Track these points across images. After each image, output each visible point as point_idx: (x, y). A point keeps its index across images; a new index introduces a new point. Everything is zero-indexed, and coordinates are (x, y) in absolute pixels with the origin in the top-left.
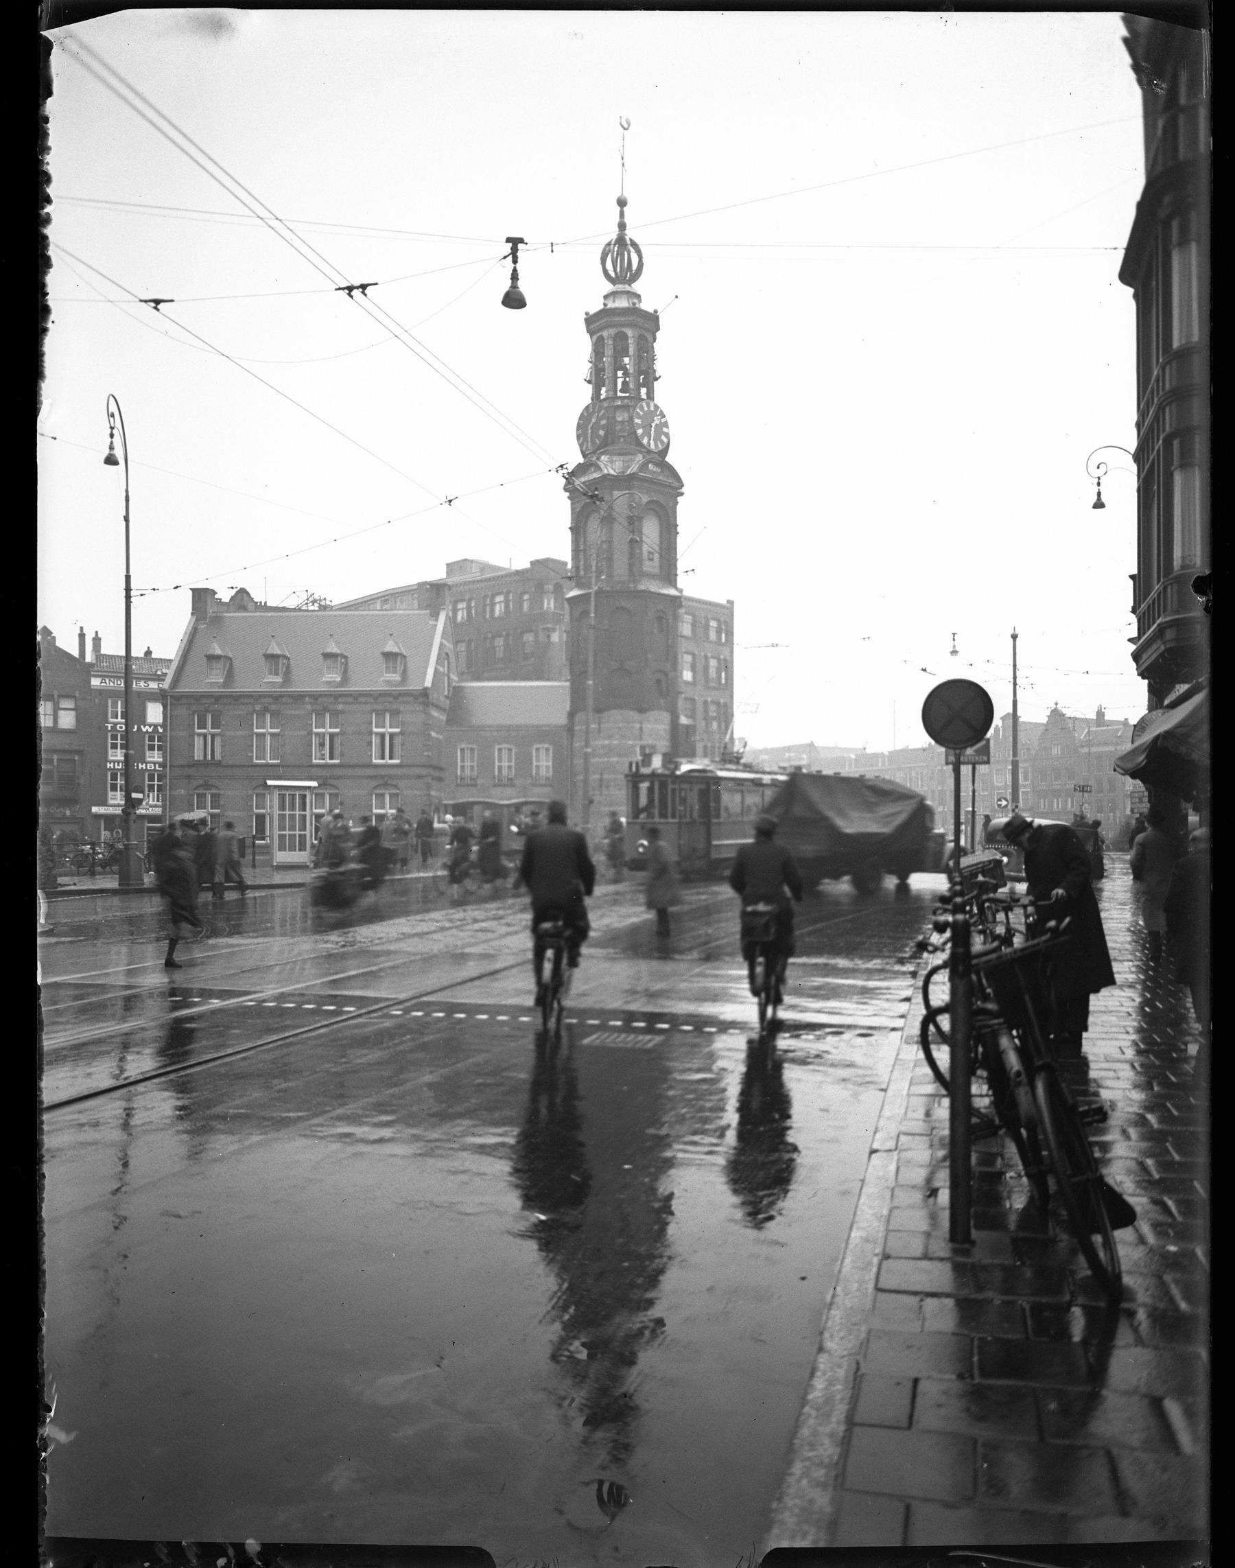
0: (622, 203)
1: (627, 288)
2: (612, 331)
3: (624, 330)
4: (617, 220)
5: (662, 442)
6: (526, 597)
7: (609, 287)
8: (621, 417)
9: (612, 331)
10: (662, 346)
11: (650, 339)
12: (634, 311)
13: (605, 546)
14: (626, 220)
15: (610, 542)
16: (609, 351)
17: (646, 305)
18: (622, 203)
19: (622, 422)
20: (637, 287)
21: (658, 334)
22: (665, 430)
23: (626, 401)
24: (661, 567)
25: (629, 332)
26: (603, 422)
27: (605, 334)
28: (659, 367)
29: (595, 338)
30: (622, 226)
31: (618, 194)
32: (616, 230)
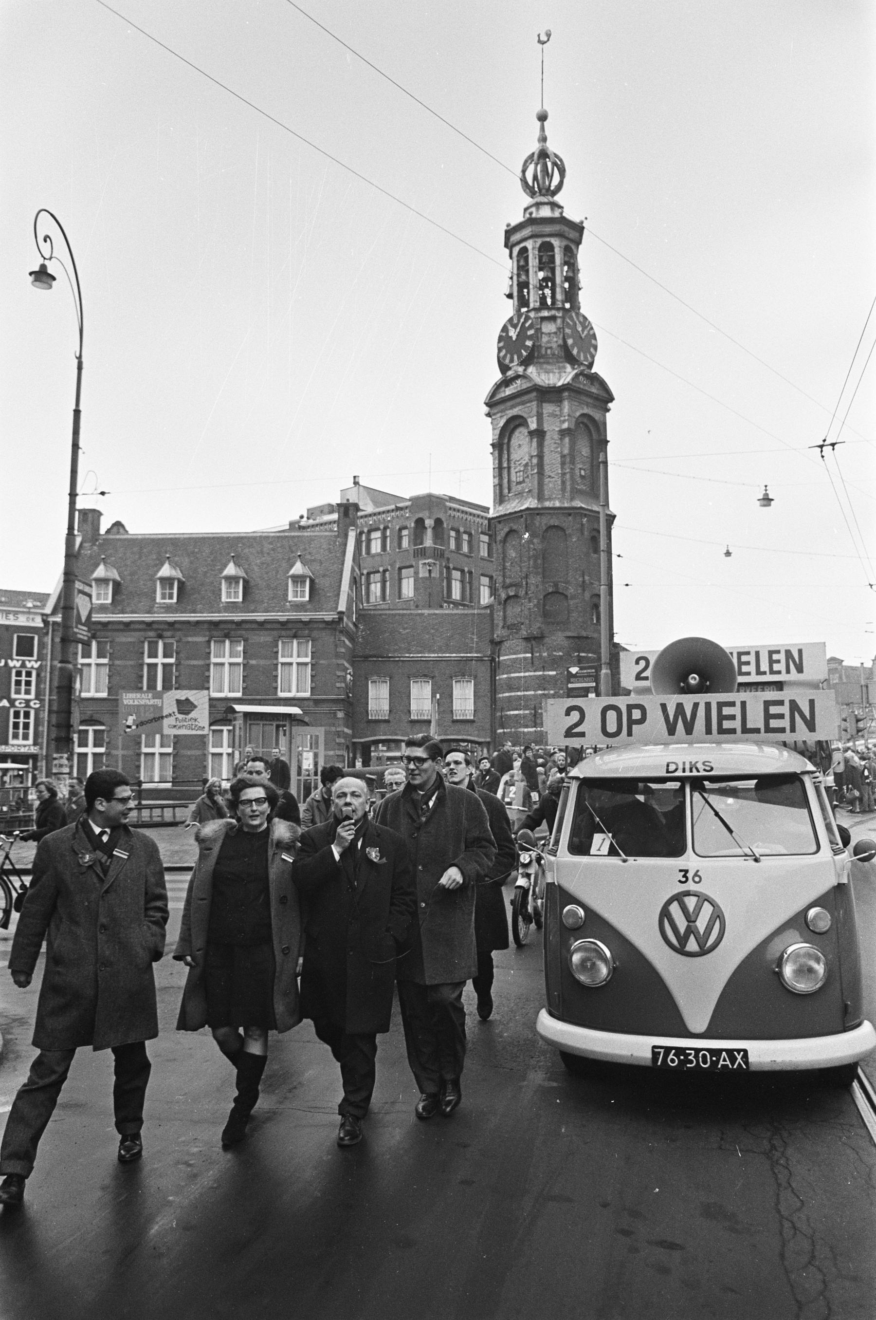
0: (542, 118)
2: (539, 241)
3: (548, 239)
4: (537, 133)
5: (591, 354)
6: (405, 532)
7: (528, 200)
8: (549, 328)
9: (539, 241)
11: (575, 250)
12: (563, 220)
13: (535, 461)
14: (547, 133)
15: (540, 457)
16: (533, 262)
18: (542, 118)
19: (549, 334)
20: (557, 198)
21: (580, 247)
22: (593, 342)
23: (553, 312)
25: (556, 242)
26: (531, 332)
27: (529, 244)
28: (583, 278)
29: (516, 250)
30: (543, 139)
31: (537, 109)
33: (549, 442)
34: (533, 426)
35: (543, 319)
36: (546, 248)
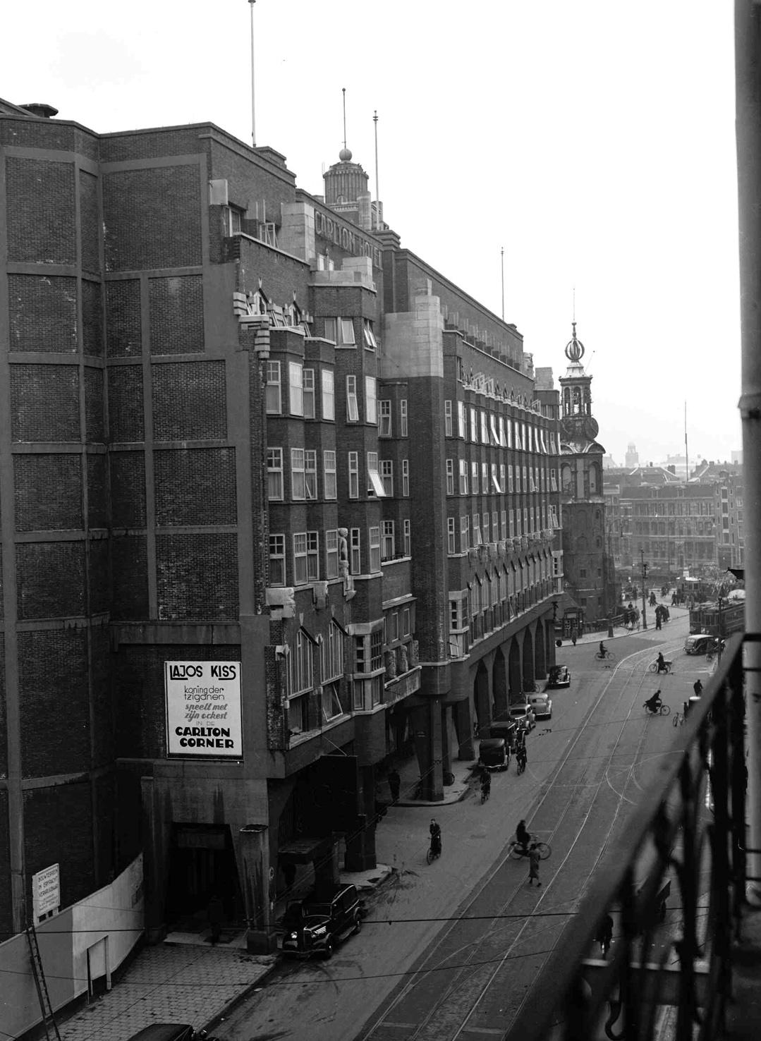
0: (574, 324)
1: (574, 364)
2: (574, 387)
7: (568, 362)
8: (578, 424)
9: (574, 387)
10: (592, 387)
15: (576, 482)
17: (588, 375)
18: (574, 324)
23: (580, 418)
24: (597, 488)
25: (581, 387)
27: (570, 388)
29: (564, 388)
30: (574, 335)
32: (572, 337)
33: (578, 475)
34: (573, 470)
35: (576, 420)
36: (577, 390)
